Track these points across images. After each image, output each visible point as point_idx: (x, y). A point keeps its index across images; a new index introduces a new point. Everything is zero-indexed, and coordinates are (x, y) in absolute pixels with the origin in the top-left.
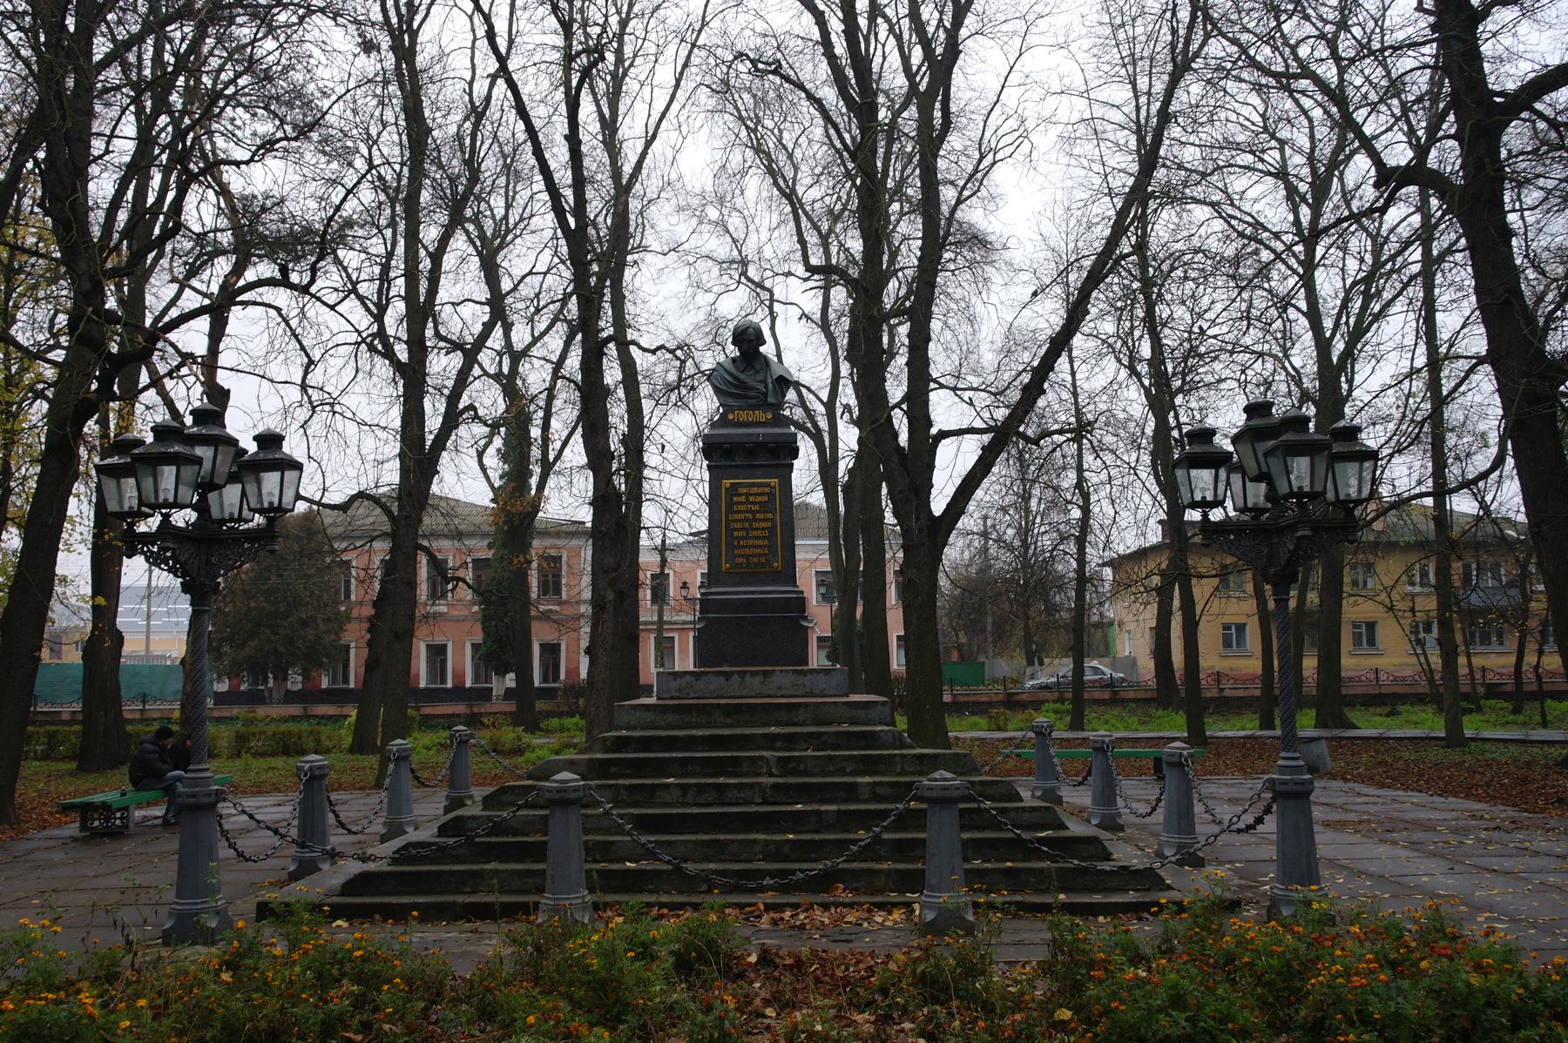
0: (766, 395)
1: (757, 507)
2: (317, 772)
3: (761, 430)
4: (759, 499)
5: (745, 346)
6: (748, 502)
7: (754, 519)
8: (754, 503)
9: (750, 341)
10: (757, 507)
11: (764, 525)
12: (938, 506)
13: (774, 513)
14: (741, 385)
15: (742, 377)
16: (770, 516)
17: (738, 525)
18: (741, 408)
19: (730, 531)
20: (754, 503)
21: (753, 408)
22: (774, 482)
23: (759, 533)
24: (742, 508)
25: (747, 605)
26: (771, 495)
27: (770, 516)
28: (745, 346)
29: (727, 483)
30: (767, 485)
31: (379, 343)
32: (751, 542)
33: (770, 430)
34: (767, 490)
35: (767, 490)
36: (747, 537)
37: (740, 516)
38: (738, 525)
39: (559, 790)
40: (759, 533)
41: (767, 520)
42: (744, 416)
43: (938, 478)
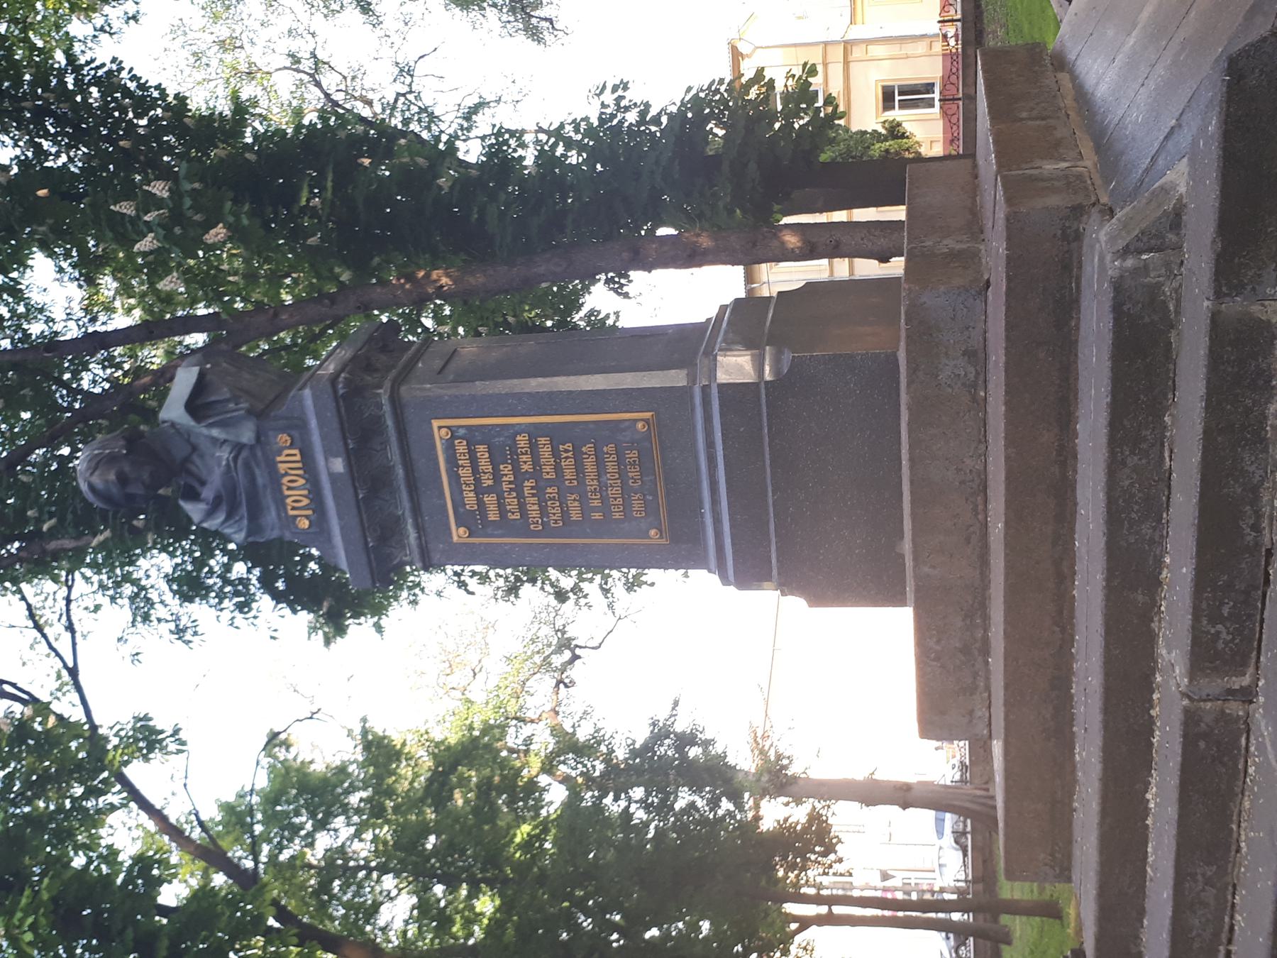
0: (238, 448)
1: (506, 469)
4: (484, 463)
6: (495, 489)
7: (537, 473)
8: (497, 476)
10: (506, 469)
11: (545, 452)
16: (522, 440)
17: (555, 511)
18: (280, 501)
20: (497, 476)
21: (275, 478)
22: (439, 429)
23: (568, 465)
24: (512, 502)
27: (522, 440)
29: (458, 534)
32: (591, 484)
33: (316, 438)
34: (461, 447)
35: (461, 447)
37: (533, 511)
38: (555, 511)
40: (568, 465)
41: (533, 446)
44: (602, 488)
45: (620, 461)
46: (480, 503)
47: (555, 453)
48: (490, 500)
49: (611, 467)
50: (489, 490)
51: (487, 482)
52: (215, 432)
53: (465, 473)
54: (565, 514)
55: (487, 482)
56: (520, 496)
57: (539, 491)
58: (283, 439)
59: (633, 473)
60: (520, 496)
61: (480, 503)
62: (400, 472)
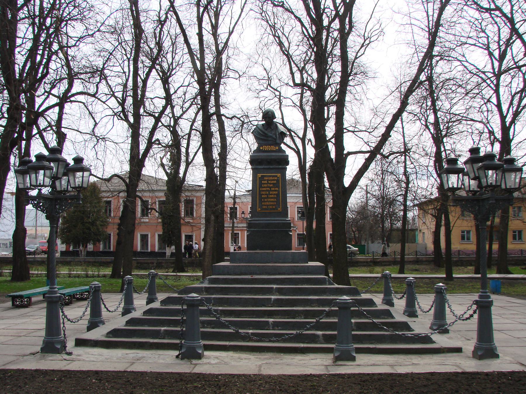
0: (276, 139)
1: (272, 185)
2: (97, 289)
3: (273, 154)
4: (272, 182)
5: (267, 119)
6: (268, 183)
7: (271, 190)
8: (271, 184)
9: (269, 118)
10: (272, 185)
11: (275, 193)
12: (347, 181)
13: (279, 188)
14: (265, 135)
15: (266, 132)
16: (277, 189)
17: (264, 193)
19: (260, 195)
20: (271, 184)
21: (270, 145)
22: (279, 175)
24: (265, 185)
25: (268, 225)
26: (278, 181)
27: (277, 189)
28: (267, 119)
29: (259, 175)
30: (276, 176)
31: (123, 115)
32: (269, 200)
33: (277, 154)
34: (276, 178)
35: (276, 178)
36: (268, 198)
38: (264, 193)
39: (191, 300)
41: (276, 191)
42: (266, 148)
43: (347, 170)
44: (268, 202)
45: (273, 205)
46: (265, 180)
47: (274, 194)
48: (266, 182)
49: (272, 203)
50: (268, 182)
51: (269, 182)
52: (278, 136)
53: (271, 178)
54: (263, 194)
55: (269, 182)
56: (267, 187)
57: (268, 191)
58: (277, 148)
59: (271, 207)
60: (267, 187)
61: (265, 180)
62: (271, 167)
